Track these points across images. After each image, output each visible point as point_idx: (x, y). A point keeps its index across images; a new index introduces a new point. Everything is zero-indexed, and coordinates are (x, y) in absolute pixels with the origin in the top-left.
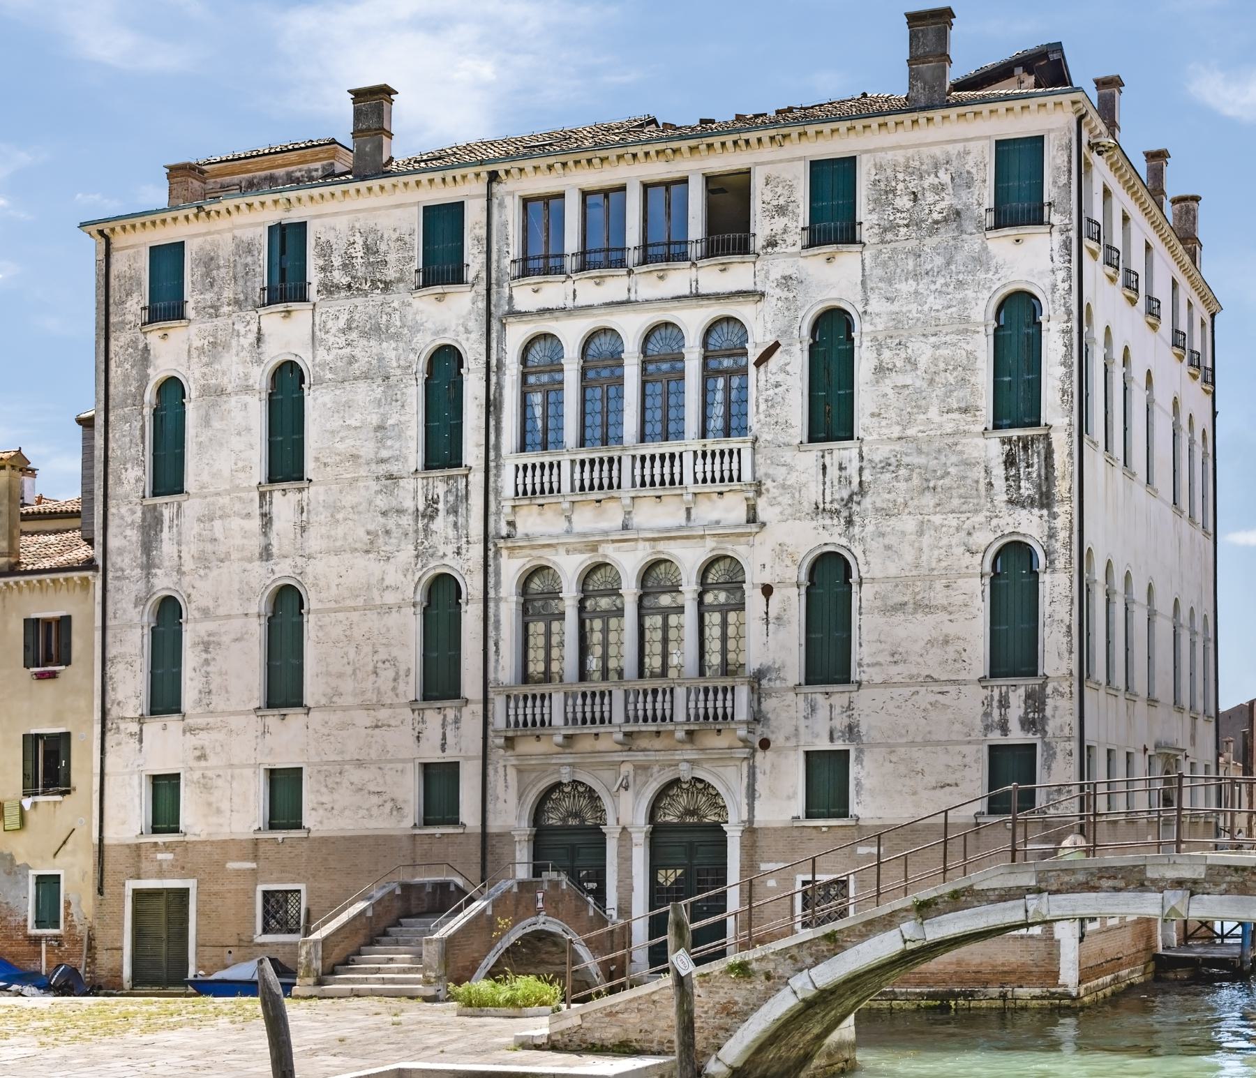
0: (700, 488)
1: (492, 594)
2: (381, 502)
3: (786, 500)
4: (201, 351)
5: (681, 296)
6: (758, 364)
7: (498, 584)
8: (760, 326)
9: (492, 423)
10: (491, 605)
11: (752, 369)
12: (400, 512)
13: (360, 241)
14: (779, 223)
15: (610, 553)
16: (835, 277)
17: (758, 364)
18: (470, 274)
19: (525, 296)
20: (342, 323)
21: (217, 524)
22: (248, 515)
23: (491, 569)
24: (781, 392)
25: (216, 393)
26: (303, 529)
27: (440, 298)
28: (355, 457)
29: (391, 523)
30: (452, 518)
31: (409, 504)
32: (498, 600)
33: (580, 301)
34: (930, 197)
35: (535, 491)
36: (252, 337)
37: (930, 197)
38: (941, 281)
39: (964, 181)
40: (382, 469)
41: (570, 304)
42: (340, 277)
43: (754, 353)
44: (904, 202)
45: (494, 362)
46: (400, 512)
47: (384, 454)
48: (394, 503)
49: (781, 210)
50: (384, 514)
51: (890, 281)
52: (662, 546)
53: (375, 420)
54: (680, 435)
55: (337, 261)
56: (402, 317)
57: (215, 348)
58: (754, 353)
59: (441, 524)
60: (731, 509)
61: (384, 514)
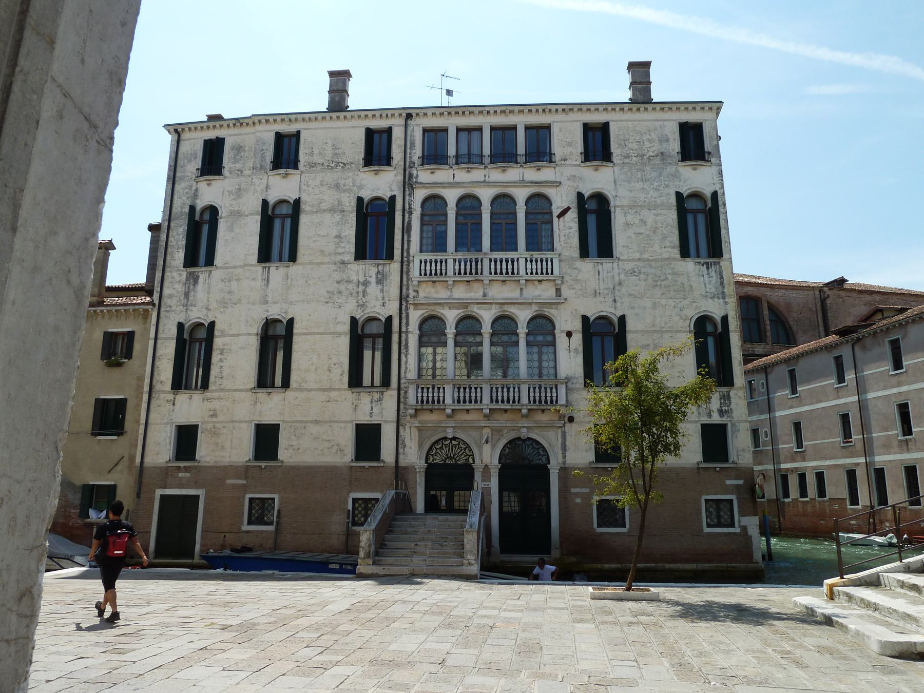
0: (529, 277)
1: (404, 329)
2: (337, 276)
3: (578, 287)
4: (230, 193)
5: (518, 180)
6: (559, 216)
7: (407, 324)
8: (561, 198)
9: (406, 238)
10: (403, 335)
11: (555, 219)
12: (349, 282)
13: (330, 142)
14: (568, 150)
15: (476, 310)
16: (598, 179)
17: (559, 216)
18: (394, 162)
19: (424, 175)
20: (318, 182)
21: (234, 283)
22: (254, 279)
23: (404, 315)
25: (237, 215)
26: (288, 288)
27: (377, 172)
28: (322, 252)
30: (380, 287)
31: (354, 278)
32: (407, 332)
33: (457, 179)
34: (647, 144)
35: (435, 274)
36: (263, 186)
37: (647, 144)
38: (656, 184)
39: (665, 140)
40: (338, 258)
41: (451, 181)
42: (317, 159)
43: (556, 212)
45: (407, 206)
46: (349, 282)
47: (340, 250)
48: (345, 277)
49: (570, 144)
50: (338, 282)
51: (629, 182)
52: (506, 308)
53: (335, 233)
55: (316, 151)
56: (354, 181)
57: (239, 192)
58: (556, 212)
59: (373, 289)
60: (546, 292)
61: (338, 282)
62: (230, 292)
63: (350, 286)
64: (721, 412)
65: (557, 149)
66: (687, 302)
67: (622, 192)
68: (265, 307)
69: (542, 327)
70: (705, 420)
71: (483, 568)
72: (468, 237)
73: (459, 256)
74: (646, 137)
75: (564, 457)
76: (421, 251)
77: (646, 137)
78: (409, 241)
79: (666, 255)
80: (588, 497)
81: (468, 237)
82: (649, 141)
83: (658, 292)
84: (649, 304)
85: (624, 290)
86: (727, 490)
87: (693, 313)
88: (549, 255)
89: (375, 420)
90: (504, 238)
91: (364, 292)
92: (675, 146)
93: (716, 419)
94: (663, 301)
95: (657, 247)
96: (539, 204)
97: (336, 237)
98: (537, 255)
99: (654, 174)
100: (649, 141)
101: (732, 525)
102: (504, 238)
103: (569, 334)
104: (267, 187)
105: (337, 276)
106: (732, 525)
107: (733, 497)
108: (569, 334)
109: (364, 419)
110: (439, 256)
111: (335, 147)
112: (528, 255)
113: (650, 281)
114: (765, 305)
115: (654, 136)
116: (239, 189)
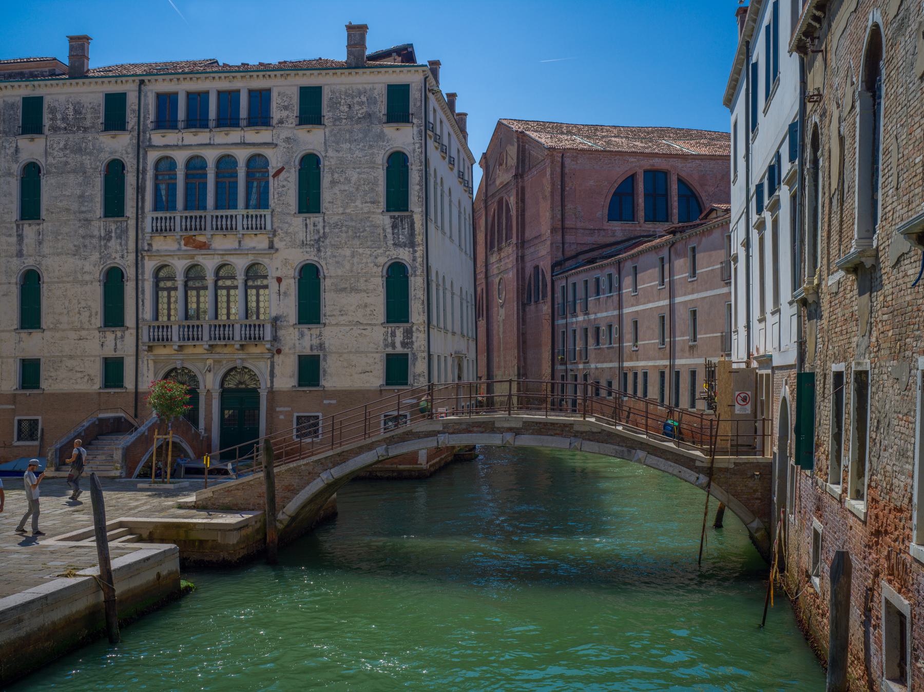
0: (245, 232)
2: (81, 231)
3: (288, 239)
6: (274, 176)
7: (143, 273)
8: (275, 159)
11: (271, 179)
12: (92, 237)
16: (312, 139)
17: (274, 176)
19: (157, 138)
20: (61, 145)
22: (10, 235)
24: (285, 190)
26: (40, 243)
31: (96, 233)
32: (143, 280)
34: (357, 107)
36: (12, 150)
37: (357, 107)
39: (372, 101)
43: (272, 172)
46: (92, 237)
47: (83, 209)
49: (286, 108)
50: (83, 237)
51: (337, 143)
52: (226, 258)
53: (78, 192)
55: (59, 116)
58: (272, 172)
60: (260, 242)
61: (83, 237)
63: (95, 241)
65: (276, 114)
70: (390, 350)
75: (272, 382)
79: (366, 210)
81: (195, 200)
83: (357, 242)
84: (348, 252)
85: (327, 241)
91: (105, 245)
92: (382, 108)
93: (399, 349)
94: (361, 251)
95: (358, 203)
96: (257, 165)
99: (361, 135)
104: (17, 150)
105: (81, 231)
112: (244, 212)
113: (350, 233)
115: (364, 99)
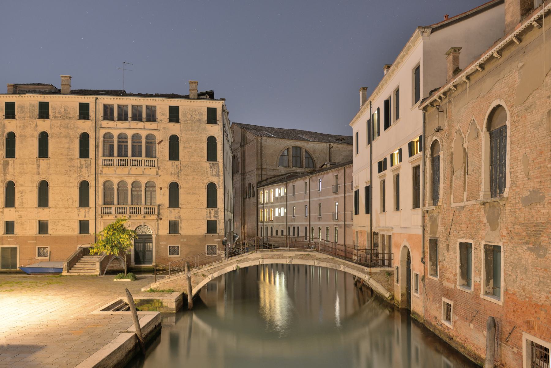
0: (146, 167)
2: (69, 164)
3: (165, 171)
4: (20, 127)
5: (142, 129)
6: (158, 144)
7: (98, 183)
8: (159, 137)
11: (157, 145)
12: (74, 166)
13: (63, 108)
15: (125, 179)
16: (175, 129)
17: (158, 144)
19: (105, 124)
20: (59, 125)
21: (25, 165)
22: (33, 164)
24: (163, 150)
25: (24, 137)
26: (48, 168)
28: (62, 154)
29: (71, 169)
31: (76, 165)
32: (98, 187)
34: (194, 116)
36: (34, 125)
37: (194, 116)
39: (201, 114)
40: (69, 157)
42: (57, 115)
43: (157, 142)
44: (189, 116)
46: (74, 166)
47: (70, 154)
49: (163, 114)
50: (70, 167)
51: (186, 131)
52: (137, 178)
53: (67, 146)
54: (140, 156)
55: (57, 111)
56: (74, 125)
57: (24, 127)
58: (157, 142)
59: (84, 170)
61: (70, 167)
62: (23, 169)
63: (75, 168)
64: (215, 217)
65: (159, 116)
66: (205, 178)
67: (183, 135)
68: (39, 176)
69: (150, 186)
70: (209, 219)
71: (102, 273)
72: (122, 152)
73: (119, 158)
74: (194, 113)
75: (158, 232)
76: (104, 156)
77: (194, 113)
78: (98, 151)
79: (199, 160)
80: (166, 245)
81: (122, 152)
82: (195, 115)
83: (195, 173)
84: (191, 178)
85: (182, 173)
86: (214, 242)
87: (207, 182)
88: (153, 159)
89: (86, 219)
90: (137, 152)
91: (80, 171)
92: (205, 117)
93: (213, 219)
94: (196, 177)
95: (195, 157)
96: (150, 139)
97: (68, 148)
98: (148, 159)
99: (196, 128)
100: (195, 115)
101: (216, 254)
102: (137, 152)
103: (161, 189)
104: (36, 126)
105: (69, 164)
106: (216, 254)
107: (216, 245)
108: (161, 189)
109: (83, 219)
110: (110, 158)
111: (65, 110)
112: (146, 159)
113: (192, 169)
114: (304, 150)
115: (197, 113)
116: (24, 126)
